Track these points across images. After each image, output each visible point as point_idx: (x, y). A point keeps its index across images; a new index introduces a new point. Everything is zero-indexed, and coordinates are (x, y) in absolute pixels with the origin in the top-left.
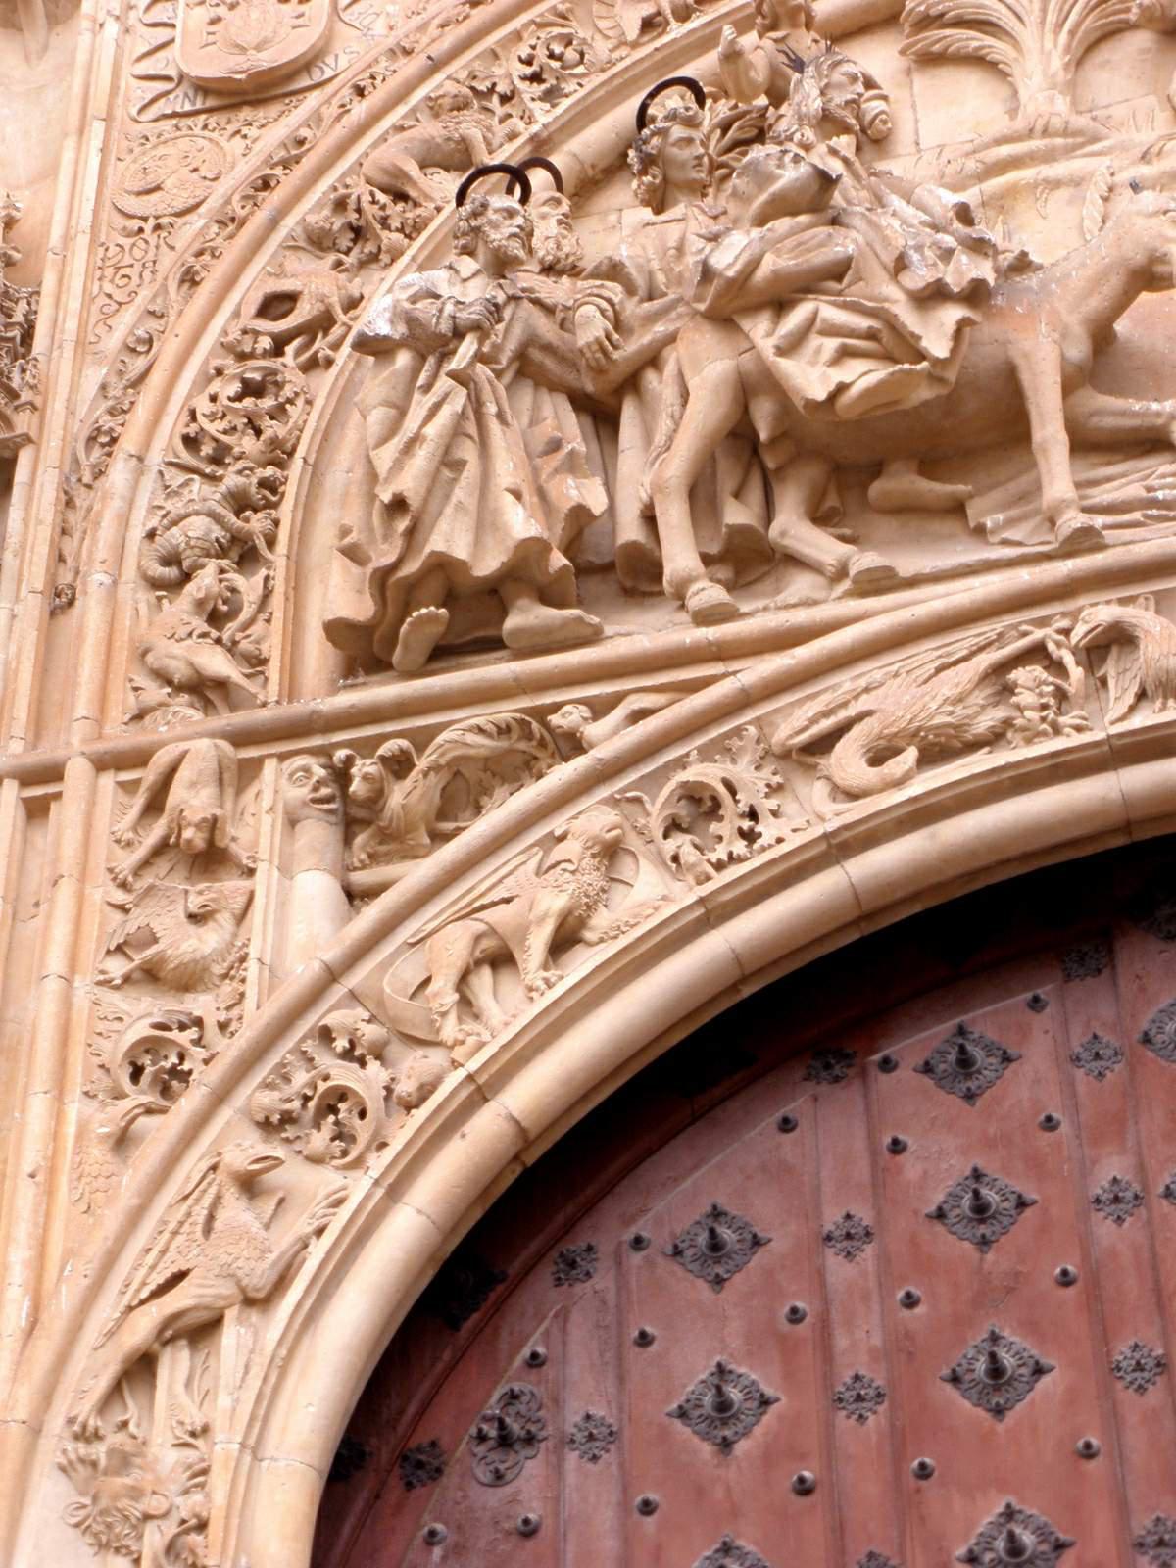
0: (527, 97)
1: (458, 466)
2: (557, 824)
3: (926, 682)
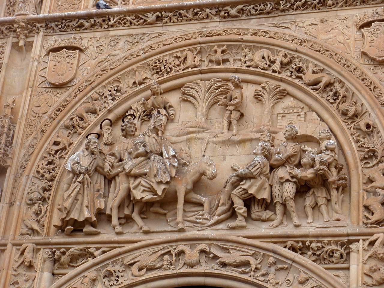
0: (109, 99)
1: (77, 200)
2: (86, 274)
3: (150, 255)
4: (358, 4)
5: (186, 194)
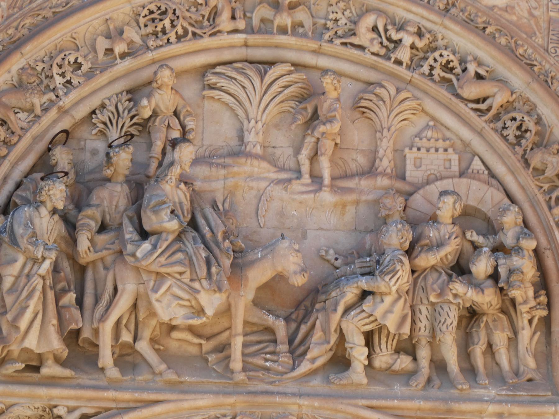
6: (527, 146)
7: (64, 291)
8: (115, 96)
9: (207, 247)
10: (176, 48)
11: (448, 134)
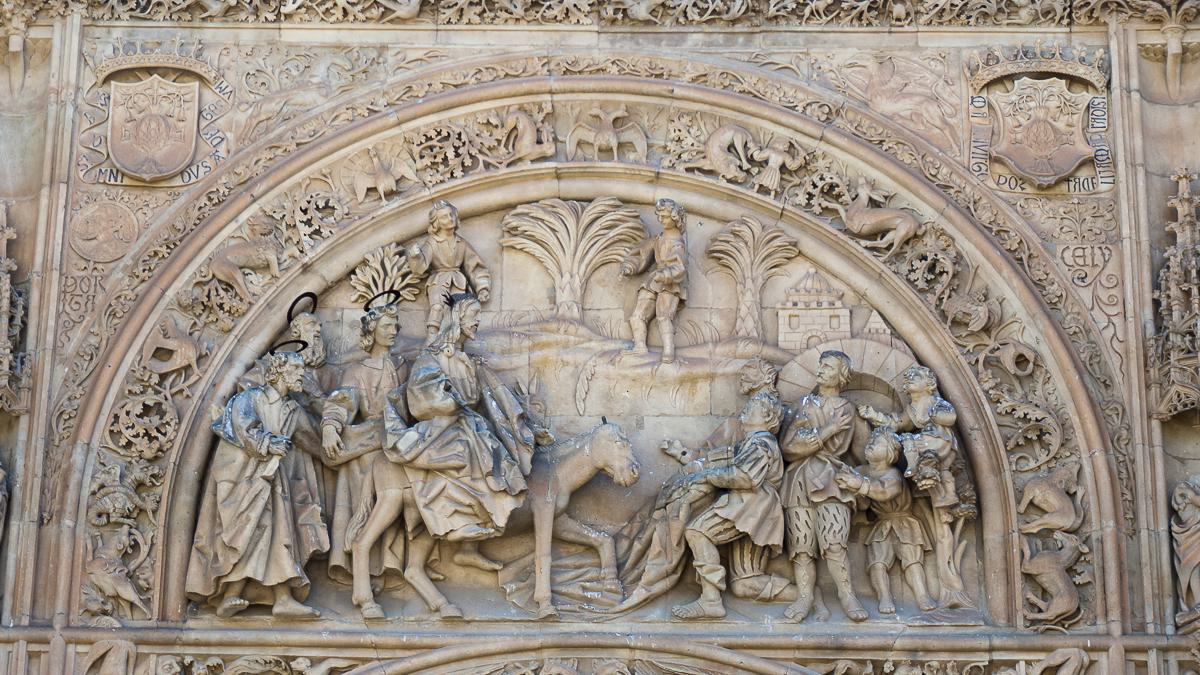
4: (972, 21)
5: (556, 517)
6: (943, 292)
7: (304, 502)
8: (380, 250)
9: (496, 433)
10: (461, 181)
11: (836, 284)
